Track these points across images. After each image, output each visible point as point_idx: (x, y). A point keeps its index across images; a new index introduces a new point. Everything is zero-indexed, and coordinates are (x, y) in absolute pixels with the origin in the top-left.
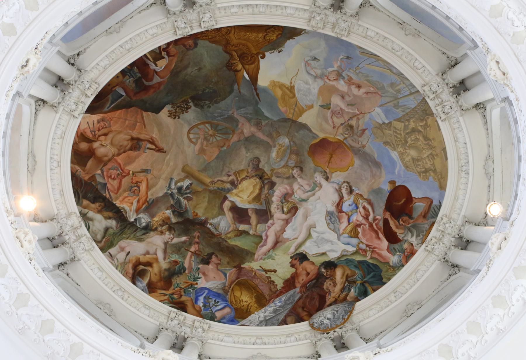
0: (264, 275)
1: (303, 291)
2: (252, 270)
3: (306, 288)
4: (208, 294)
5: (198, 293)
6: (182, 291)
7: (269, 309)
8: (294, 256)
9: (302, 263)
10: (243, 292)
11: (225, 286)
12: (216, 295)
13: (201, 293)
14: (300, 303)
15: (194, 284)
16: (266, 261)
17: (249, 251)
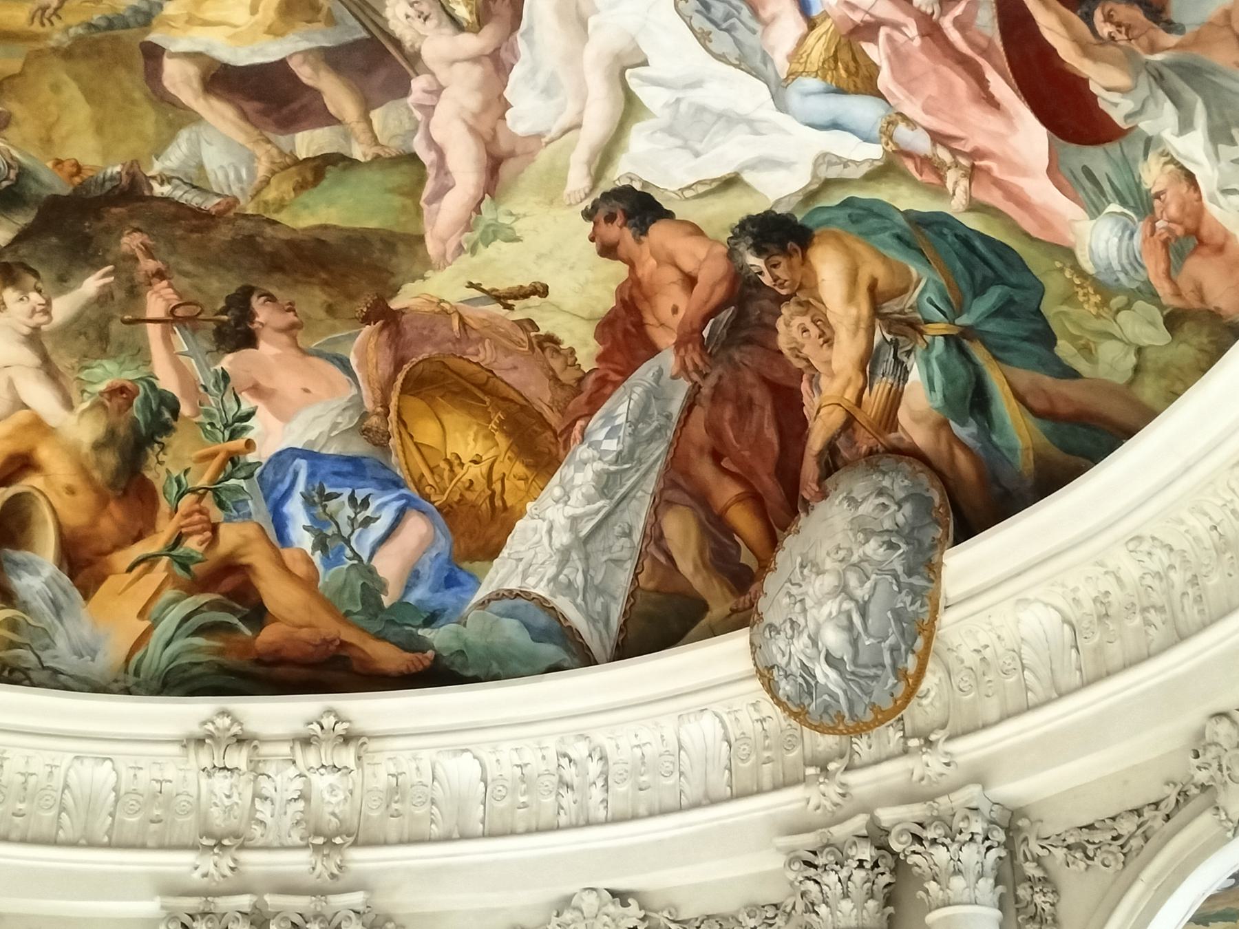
0: (503, 318)
1: (696, 365)
2: (442, 312)
3: (703, 347)
4: (311, 476)
5: (274, 485)
6: (209, 502)
7: (579, 478)
8: (595, 206)
9: (644, 233)
10: (446, 418)
11: (364, 416)
12: (347, 468)
13: (282, 481)
14: (698, 429)
15: (238, 452)
16: (486, 253)
17: (392, 234)
